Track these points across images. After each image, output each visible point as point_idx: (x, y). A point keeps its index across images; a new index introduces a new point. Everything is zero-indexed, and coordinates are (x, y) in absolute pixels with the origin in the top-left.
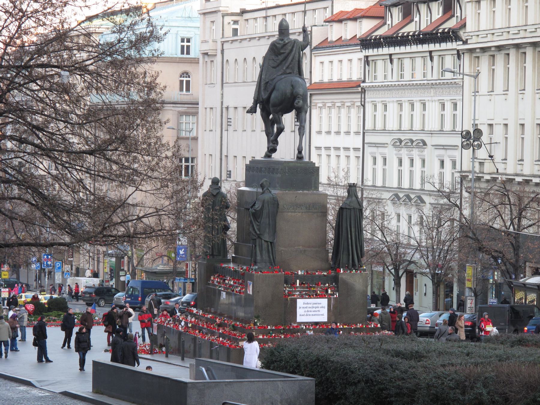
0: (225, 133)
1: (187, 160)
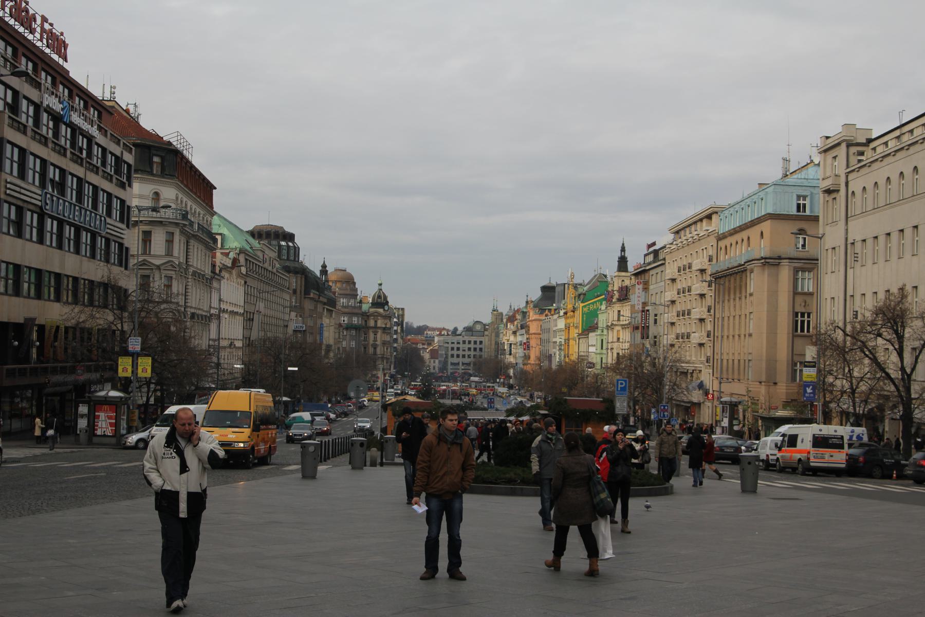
0: (850, 272)
1: (803, 315)
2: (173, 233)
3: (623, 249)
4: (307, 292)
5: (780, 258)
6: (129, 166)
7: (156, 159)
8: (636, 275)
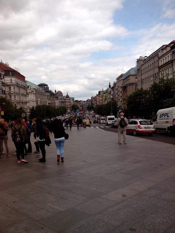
2: (15, 87)
3: (110, 83)
4: (51, 96)
5: (132, 83)
6: (3, 75)
7: (10, 73)
8: (112, 88)
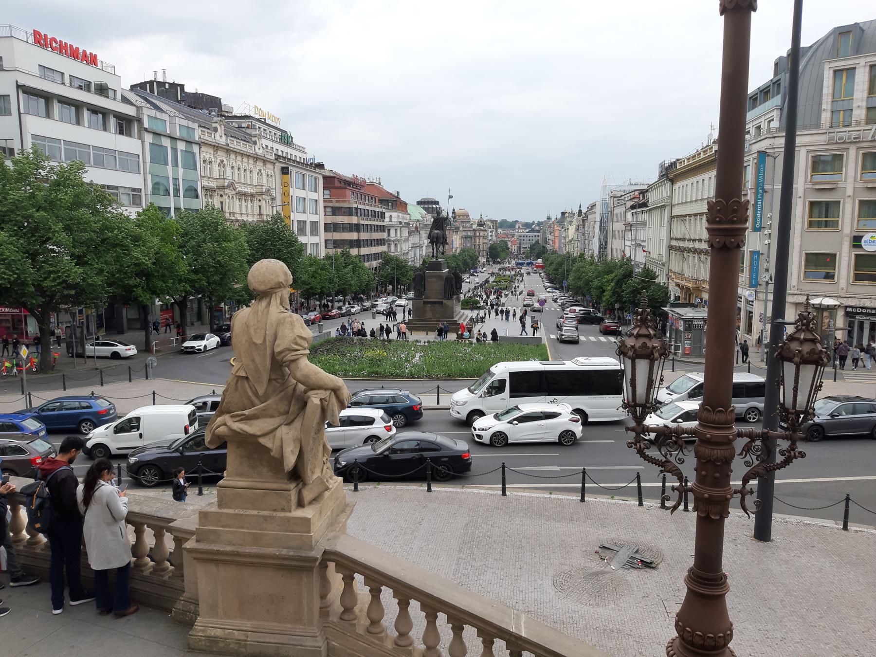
3: (580, 207)
7: (390, 204)
